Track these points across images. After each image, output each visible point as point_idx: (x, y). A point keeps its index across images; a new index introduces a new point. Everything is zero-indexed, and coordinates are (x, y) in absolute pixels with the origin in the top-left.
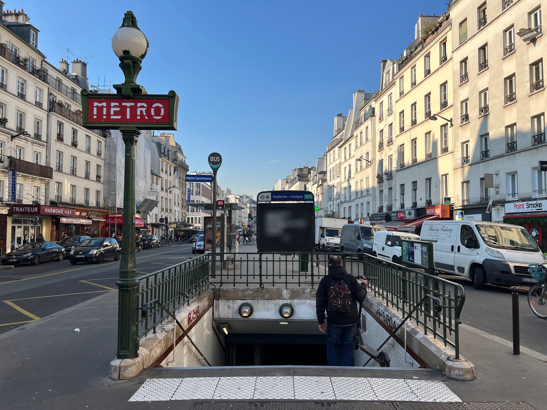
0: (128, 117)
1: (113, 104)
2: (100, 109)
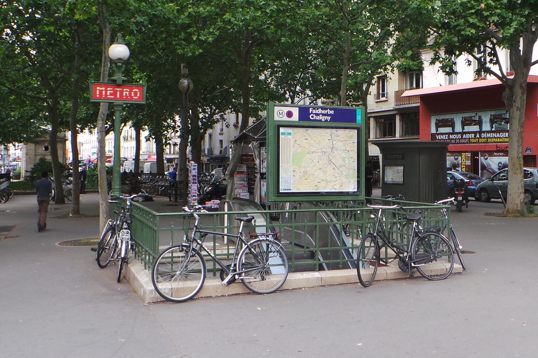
0: (118, 96)
1: (108, 89)
2: (101, 92)
